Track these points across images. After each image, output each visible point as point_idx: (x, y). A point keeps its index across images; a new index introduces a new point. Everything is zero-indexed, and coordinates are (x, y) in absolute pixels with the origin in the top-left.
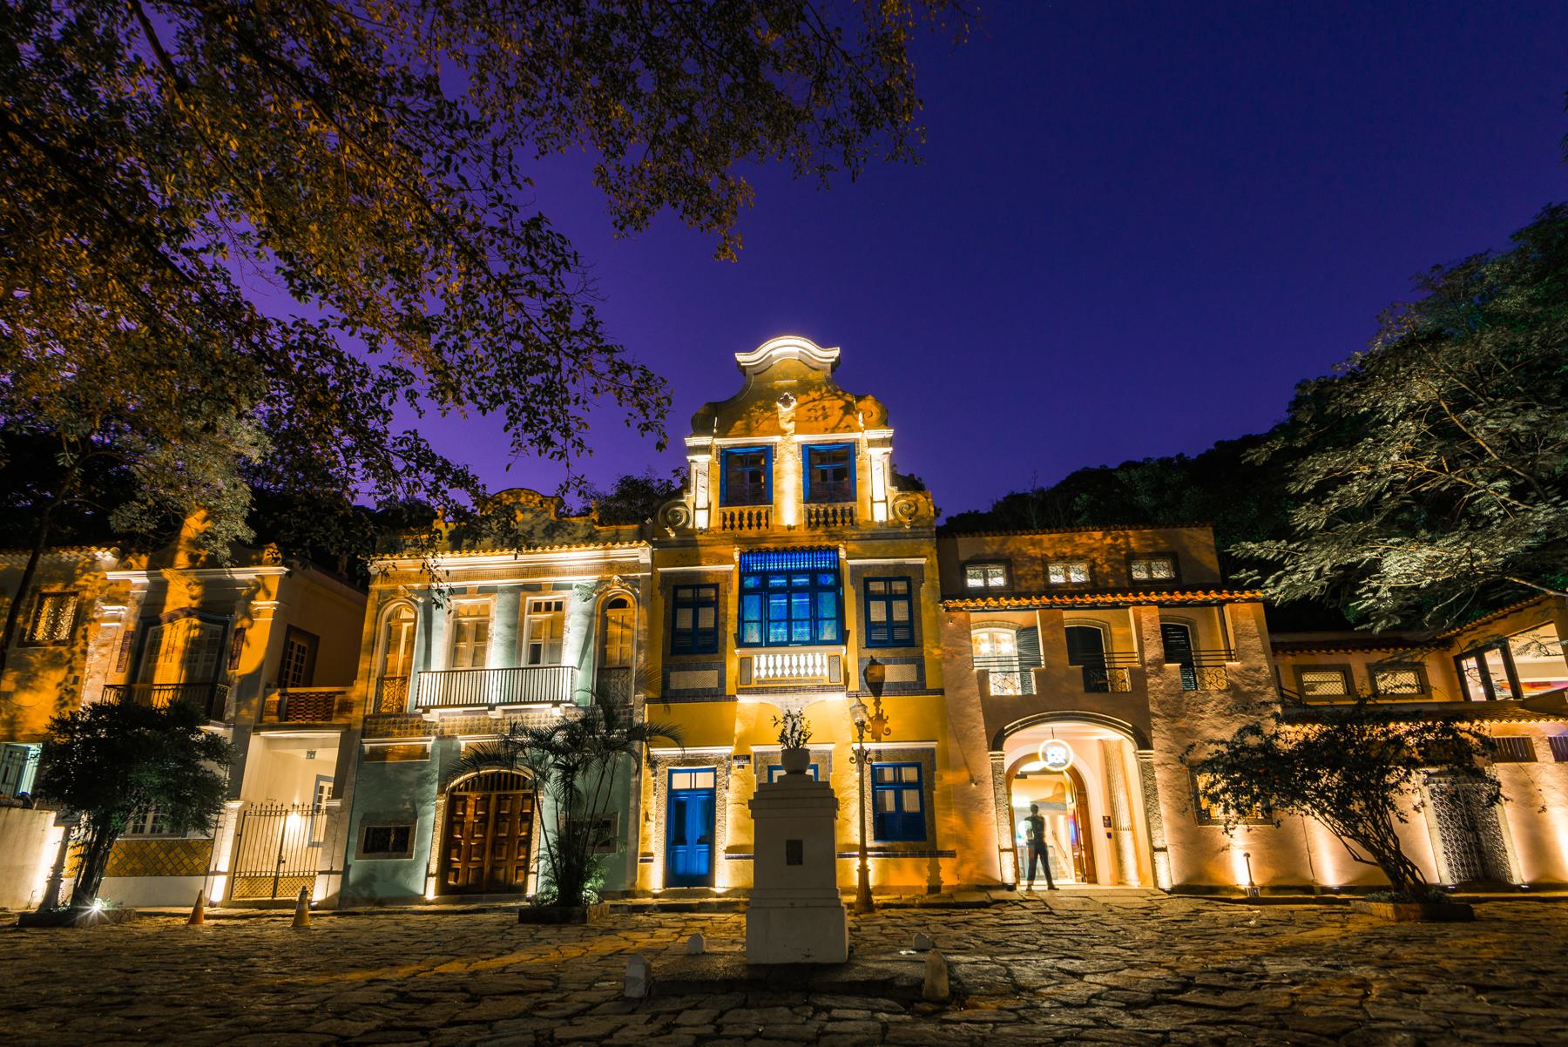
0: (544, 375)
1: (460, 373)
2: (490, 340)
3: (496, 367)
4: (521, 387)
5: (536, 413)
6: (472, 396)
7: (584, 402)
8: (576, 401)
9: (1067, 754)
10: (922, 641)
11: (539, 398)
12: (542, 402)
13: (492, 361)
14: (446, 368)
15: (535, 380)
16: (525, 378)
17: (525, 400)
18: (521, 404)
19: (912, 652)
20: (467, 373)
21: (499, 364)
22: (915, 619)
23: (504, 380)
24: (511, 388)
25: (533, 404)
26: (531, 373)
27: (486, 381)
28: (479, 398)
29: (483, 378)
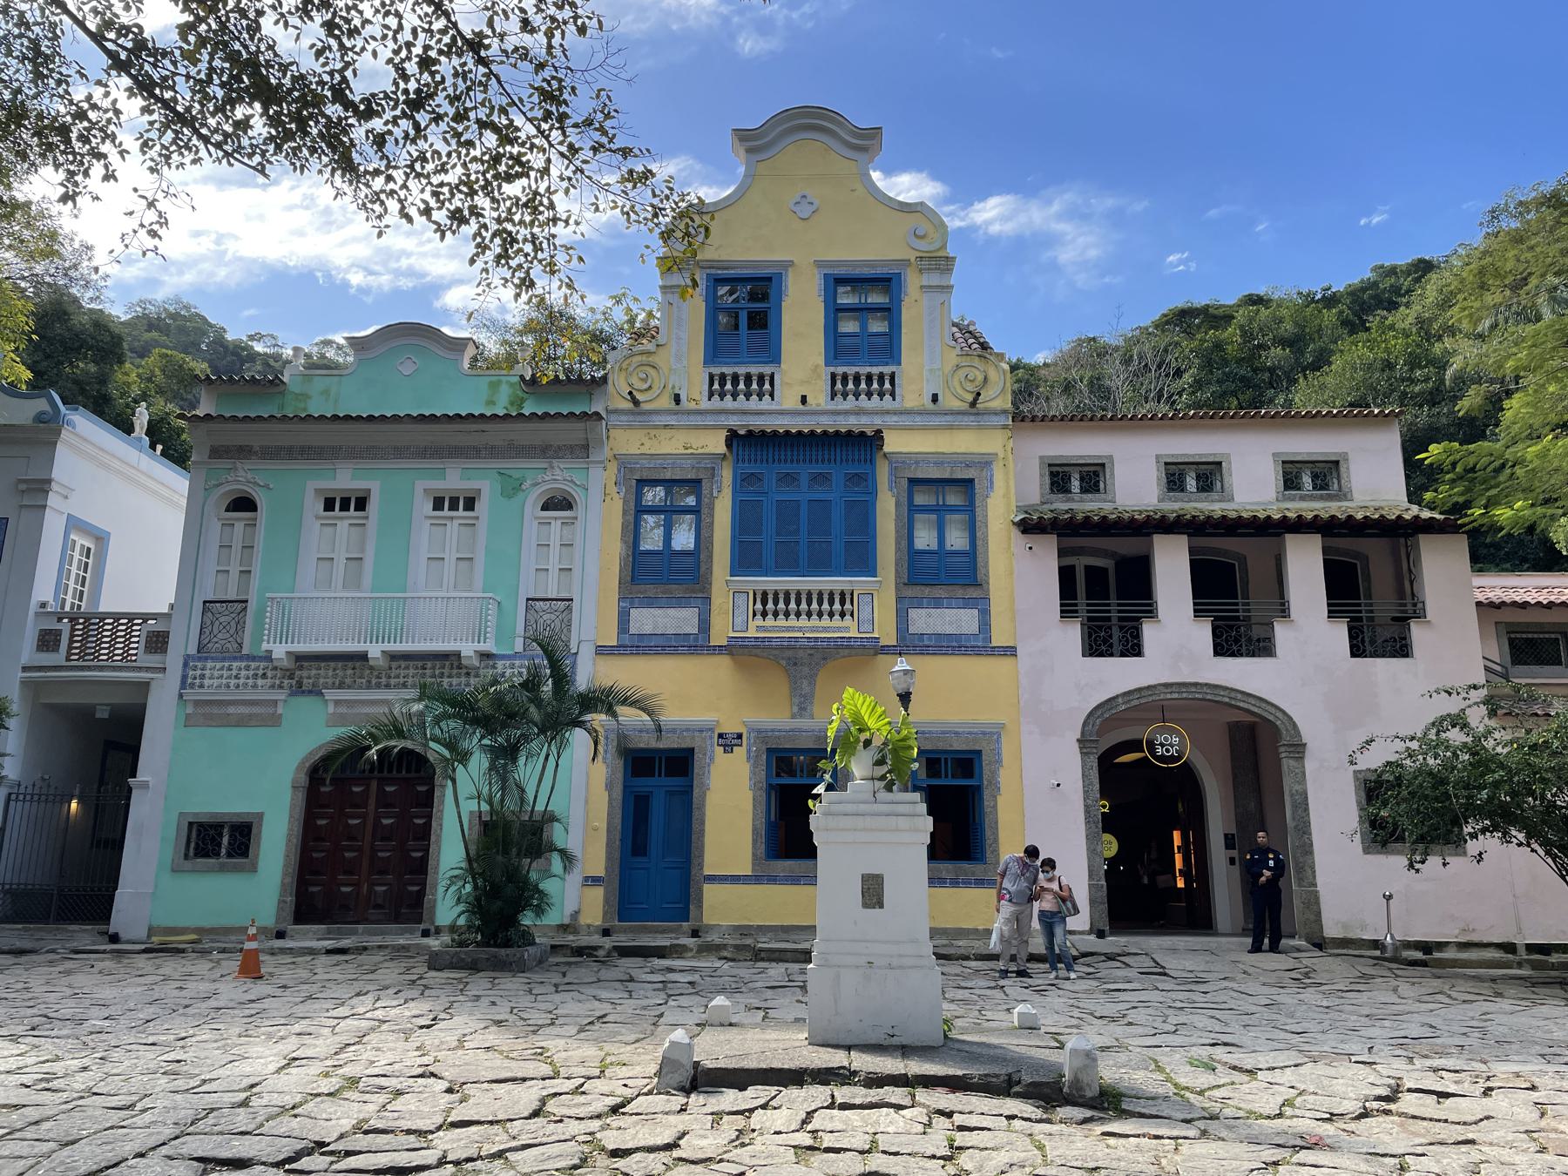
0: (524, 181)
1: (407, 175)
2: (453, 129)
3: (459, 170)
4: (494, 200)
5: (514, 241)
6: (427, 212)
7: (577, 223)
8: (567, 222)
9: (1182, 743)
10: (987, 575)
11: (517, 218)
12: (522, 222)
13: (454, 159)
14: (388, 167)
15: (514, 189)
16: (500, 187)
17: (499, 221)
18: (494, 227)
19: (973, 593)
20: (418, 175)
21: (465, 165)
22: (979, 543)
23: (470, 188)
24: (482, 201)
25: (509, 227)
26: (509, 178)
27: (445, 190)
28: (436, 215)
29: (442, 185)
